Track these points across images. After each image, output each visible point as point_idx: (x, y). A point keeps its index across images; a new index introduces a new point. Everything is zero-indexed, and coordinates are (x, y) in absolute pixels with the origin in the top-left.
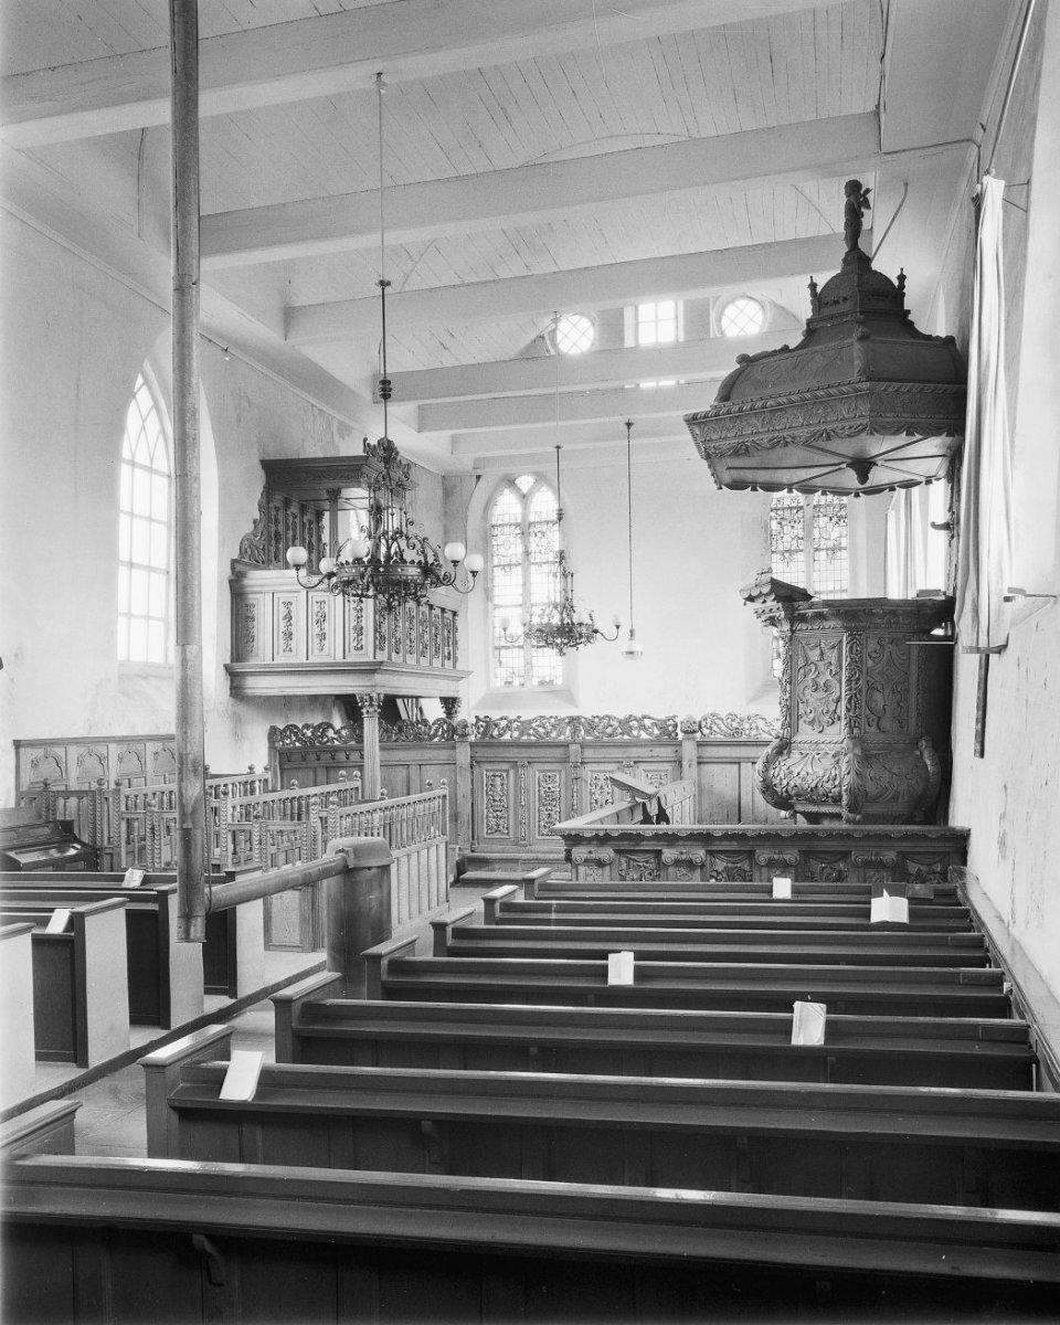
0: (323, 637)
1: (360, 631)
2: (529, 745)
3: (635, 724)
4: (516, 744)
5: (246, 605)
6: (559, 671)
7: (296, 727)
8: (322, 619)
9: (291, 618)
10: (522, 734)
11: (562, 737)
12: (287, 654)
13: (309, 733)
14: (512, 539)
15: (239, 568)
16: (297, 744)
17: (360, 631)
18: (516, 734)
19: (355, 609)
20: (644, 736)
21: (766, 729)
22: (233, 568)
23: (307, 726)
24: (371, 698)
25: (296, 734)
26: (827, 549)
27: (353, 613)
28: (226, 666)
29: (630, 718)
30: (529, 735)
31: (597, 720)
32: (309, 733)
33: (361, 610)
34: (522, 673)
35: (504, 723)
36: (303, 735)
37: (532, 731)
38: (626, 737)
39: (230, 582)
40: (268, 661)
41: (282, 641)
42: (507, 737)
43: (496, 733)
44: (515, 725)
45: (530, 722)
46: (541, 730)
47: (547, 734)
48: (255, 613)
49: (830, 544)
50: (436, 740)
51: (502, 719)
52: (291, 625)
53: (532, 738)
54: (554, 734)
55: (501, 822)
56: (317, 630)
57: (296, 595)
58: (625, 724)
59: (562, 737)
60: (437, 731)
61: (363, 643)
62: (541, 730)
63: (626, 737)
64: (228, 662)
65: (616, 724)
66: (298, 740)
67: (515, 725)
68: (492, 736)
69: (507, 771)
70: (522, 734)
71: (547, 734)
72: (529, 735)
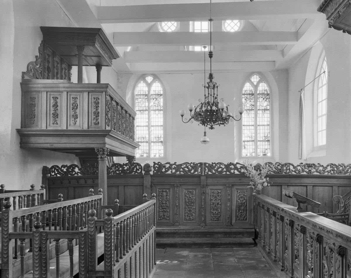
0: (76, 117)
1: (97, 114)
2: (180, 176)
3: (232, 167)
4: (173, 175)
5: (31, 98)
6: (162, 152)
7: (58, 167)
8: (75, 107)
9: (57, 106)
10: (176, 171)
11: (196, 173)
12: (55, 125)
13: (65, 170)
14: (144, 100)
15: (26, 77)
16: (58, 175)
17: (97, 114)
18: (174, 171)
19: (95, 102)
20: (236, 172)
21: (294, 170)
22: (23, 77)
23: (64, 166)
24: (104, 150)
25: (57, 170)
26: (262, 110)
27: (94, 104)
28: (18, 131)
29: (231, 164)
30: (180, 171)
31: (214, 165)
32: (65, 170)
33: (98, 103)
34: (147, 151)
35: (168, 166)
36: (62, 171)
37: (181, 170)
38: (228, 173)
39: (21, 84)
40: (44, 128)
41: (52, 119)
42: (169, 172)
43: (164, 170)
44: (173, 166)
45: (181, 165)
46: (186, 169)
47: (190, 171)
48: (36, 102)
49: (263, 108)
50: (133, 173)
51: (167, 163)
52: (57, 110)
53: (182, 173)
54: (192, 171)
55: (165, 214)
56: (73, 113)
57: (61, 93)
58: (228, 166)
59: (196, 173)
60: (133, 169)
61: (99, 120)
62: (186, 169)
63: (228, 173)
64: (19, 128)
65: (223, 167)
66: (59, 173)
67: (173, 166)
68: (162, 172)
69: (169, 189)
70: (176, 171)
71: (190, 171)
72: (180, 171)
